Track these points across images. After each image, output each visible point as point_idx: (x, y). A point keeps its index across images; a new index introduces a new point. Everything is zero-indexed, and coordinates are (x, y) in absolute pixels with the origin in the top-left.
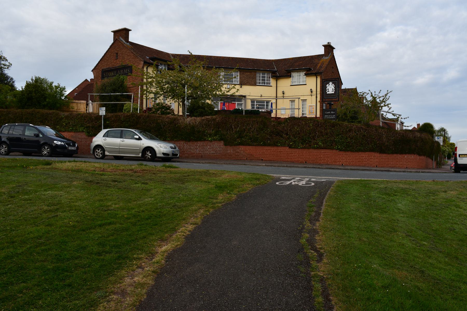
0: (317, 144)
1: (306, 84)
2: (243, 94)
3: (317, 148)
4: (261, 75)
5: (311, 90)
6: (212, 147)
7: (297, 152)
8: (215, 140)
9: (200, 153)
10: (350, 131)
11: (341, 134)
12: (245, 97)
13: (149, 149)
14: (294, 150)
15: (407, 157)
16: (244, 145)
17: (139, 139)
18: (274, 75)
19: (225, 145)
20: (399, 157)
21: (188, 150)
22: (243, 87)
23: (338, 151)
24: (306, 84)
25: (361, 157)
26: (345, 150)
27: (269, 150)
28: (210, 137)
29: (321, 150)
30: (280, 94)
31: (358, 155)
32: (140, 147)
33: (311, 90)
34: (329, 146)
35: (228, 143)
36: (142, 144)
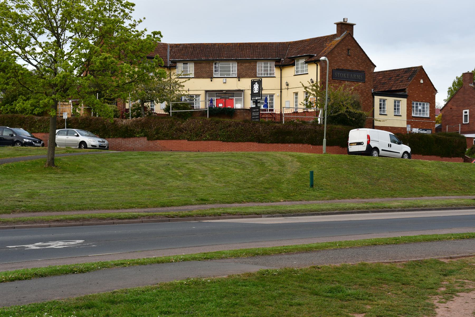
0: (206, 137)
1: (308, 74)
2: (242, 89)
3: (205, 140)
4: (263, 65)
5: (311, 80)
6: (140, 142)
7: (192, 143)
8: (141, 136)
9: (132, 147)
10: (230, 126)
11: (223, 129)
12: (242, 91)
13: (83, 143)
14: (190, 142)
15: (291, 146)
16: (159, 140)
17: (78, 136)
18: (278, 64)
19: (148, 140)
20: (280, 146)
21: (124, 145)
22: (241, 79)
23: (221, 142)
24: (308, 74)
25: (241, 146)
26: (227, 141)
27: (175, 142)
28: (138, 134)
29: (209, 141)
30: (284, 86)
31: (238, 144)
32: (78, 141)
33: (311, 80)
34: (214, 138)
35: (150, 138)
36: (79, 140)
